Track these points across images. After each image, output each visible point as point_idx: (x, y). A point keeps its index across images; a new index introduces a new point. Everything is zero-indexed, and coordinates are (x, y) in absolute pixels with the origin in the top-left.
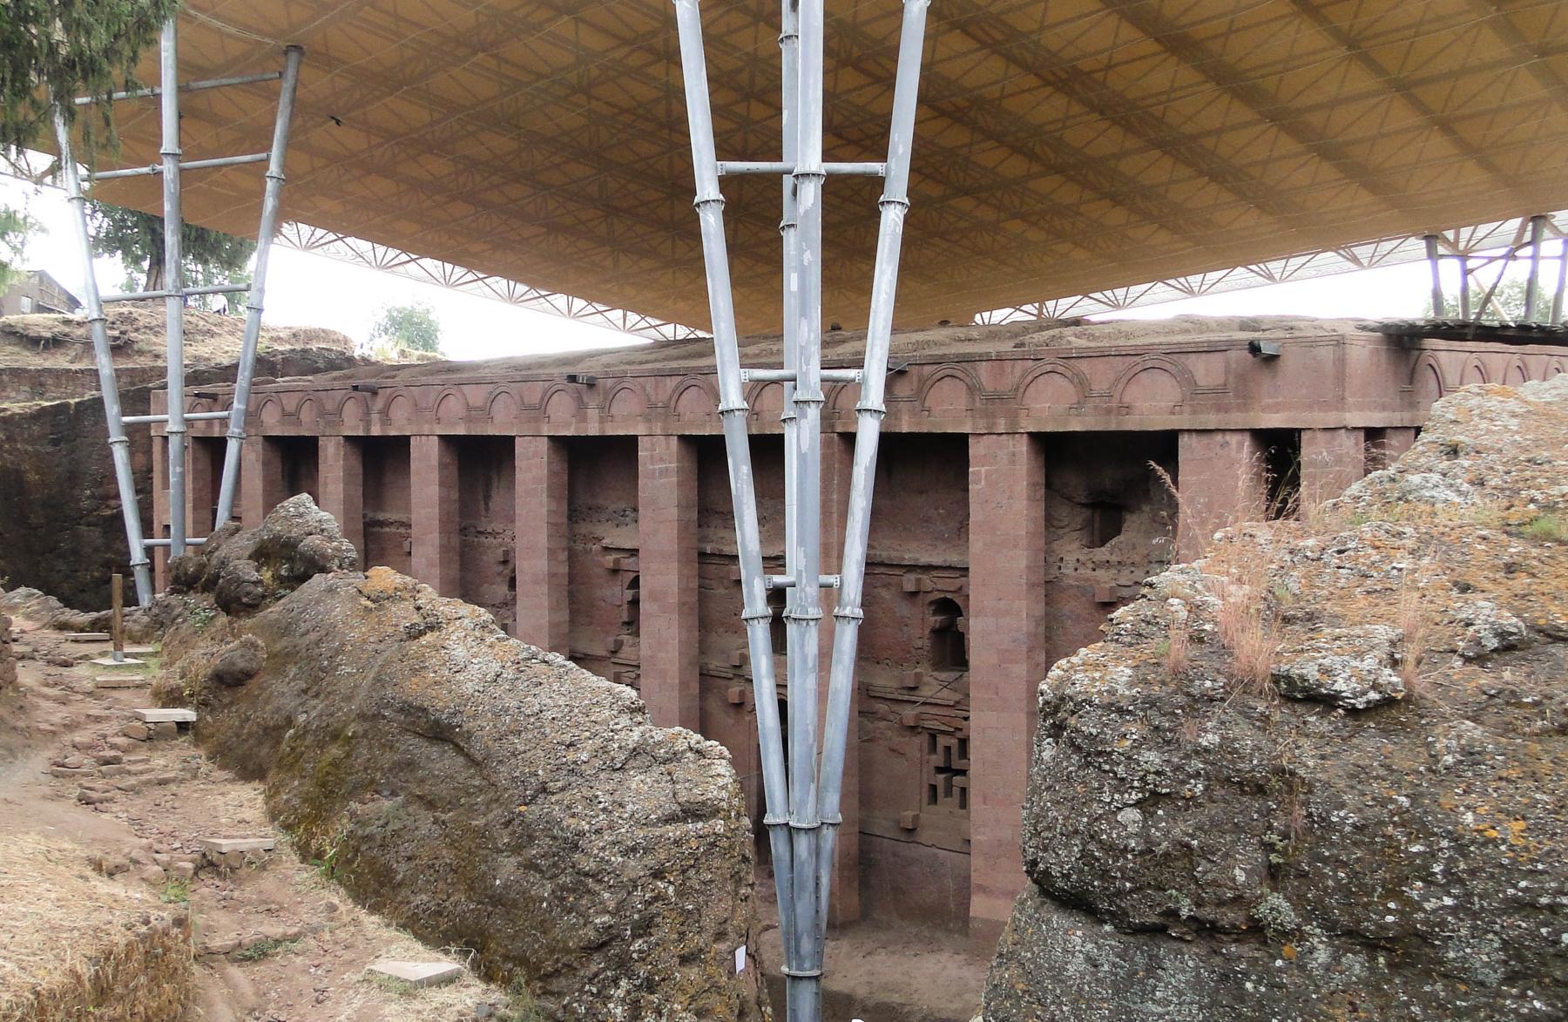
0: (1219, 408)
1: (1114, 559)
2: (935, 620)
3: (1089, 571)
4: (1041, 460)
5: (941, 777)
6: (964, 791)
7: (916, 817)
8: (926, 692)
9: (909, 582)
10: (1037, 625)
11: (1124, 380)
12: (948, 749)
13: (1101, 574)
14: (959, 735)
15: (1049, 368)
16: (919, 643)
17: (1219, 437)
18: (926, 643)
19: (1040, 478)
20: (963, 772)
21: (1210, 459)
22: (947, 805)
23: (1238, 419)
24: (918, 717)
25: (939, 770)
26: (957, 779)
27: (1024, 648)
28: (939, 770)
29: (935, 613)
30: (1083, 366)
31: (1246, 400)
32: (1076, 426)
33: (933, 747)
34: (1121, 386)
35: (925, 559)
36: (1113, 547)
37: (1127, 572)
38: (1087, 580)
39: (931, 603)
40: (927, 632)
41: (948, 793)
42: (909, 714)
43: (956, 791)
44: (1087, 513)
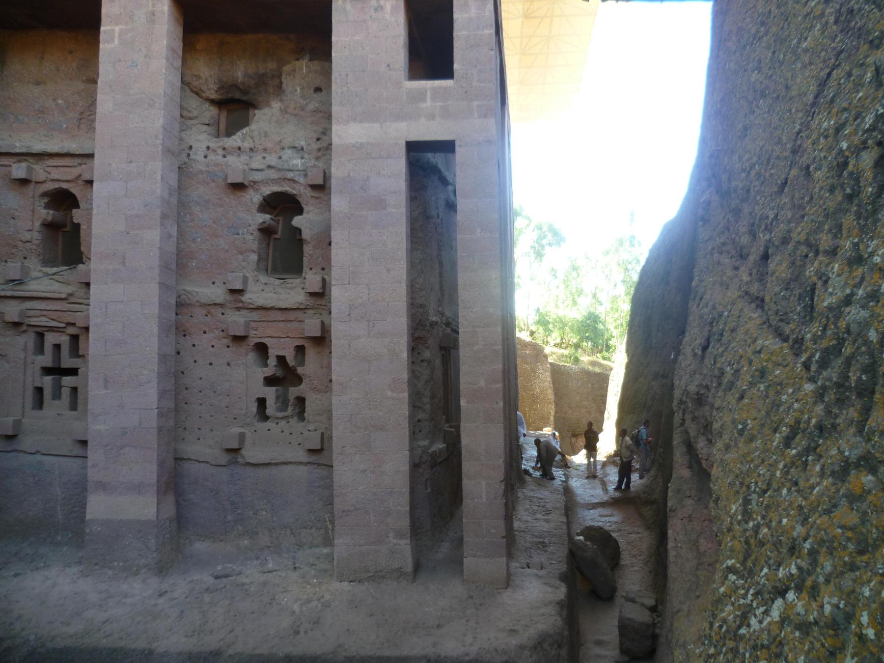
1: (246, 145)
2: (47, 214)
3: (220, 158)
4: (180, 30)
5: (48, 380)
6: (74, 390)
7: (17, 424)
8: (35, 287)
9: (19, 170)
10: (170, 194)
12: (57, 347)
13: (232, 160)
14: (72, 330)
16: (28, 236)
18: (36, 236)
19: (179, 45)
20: (73, 372)
21: (365, 21)
22: (54, 409)
24: (22, 313)
25: (47, 371)
26: (67, 381)
27: (158, 213)
28: (47, 371)
29: (47, 206)
33: (40, 349)
35: (38, 147)
36: (244, 135)
37: (259, 158)
39: (44, 195)
40: (37, 224)
41: (57, 395)
43: (66, 392)
44: (213, 111)
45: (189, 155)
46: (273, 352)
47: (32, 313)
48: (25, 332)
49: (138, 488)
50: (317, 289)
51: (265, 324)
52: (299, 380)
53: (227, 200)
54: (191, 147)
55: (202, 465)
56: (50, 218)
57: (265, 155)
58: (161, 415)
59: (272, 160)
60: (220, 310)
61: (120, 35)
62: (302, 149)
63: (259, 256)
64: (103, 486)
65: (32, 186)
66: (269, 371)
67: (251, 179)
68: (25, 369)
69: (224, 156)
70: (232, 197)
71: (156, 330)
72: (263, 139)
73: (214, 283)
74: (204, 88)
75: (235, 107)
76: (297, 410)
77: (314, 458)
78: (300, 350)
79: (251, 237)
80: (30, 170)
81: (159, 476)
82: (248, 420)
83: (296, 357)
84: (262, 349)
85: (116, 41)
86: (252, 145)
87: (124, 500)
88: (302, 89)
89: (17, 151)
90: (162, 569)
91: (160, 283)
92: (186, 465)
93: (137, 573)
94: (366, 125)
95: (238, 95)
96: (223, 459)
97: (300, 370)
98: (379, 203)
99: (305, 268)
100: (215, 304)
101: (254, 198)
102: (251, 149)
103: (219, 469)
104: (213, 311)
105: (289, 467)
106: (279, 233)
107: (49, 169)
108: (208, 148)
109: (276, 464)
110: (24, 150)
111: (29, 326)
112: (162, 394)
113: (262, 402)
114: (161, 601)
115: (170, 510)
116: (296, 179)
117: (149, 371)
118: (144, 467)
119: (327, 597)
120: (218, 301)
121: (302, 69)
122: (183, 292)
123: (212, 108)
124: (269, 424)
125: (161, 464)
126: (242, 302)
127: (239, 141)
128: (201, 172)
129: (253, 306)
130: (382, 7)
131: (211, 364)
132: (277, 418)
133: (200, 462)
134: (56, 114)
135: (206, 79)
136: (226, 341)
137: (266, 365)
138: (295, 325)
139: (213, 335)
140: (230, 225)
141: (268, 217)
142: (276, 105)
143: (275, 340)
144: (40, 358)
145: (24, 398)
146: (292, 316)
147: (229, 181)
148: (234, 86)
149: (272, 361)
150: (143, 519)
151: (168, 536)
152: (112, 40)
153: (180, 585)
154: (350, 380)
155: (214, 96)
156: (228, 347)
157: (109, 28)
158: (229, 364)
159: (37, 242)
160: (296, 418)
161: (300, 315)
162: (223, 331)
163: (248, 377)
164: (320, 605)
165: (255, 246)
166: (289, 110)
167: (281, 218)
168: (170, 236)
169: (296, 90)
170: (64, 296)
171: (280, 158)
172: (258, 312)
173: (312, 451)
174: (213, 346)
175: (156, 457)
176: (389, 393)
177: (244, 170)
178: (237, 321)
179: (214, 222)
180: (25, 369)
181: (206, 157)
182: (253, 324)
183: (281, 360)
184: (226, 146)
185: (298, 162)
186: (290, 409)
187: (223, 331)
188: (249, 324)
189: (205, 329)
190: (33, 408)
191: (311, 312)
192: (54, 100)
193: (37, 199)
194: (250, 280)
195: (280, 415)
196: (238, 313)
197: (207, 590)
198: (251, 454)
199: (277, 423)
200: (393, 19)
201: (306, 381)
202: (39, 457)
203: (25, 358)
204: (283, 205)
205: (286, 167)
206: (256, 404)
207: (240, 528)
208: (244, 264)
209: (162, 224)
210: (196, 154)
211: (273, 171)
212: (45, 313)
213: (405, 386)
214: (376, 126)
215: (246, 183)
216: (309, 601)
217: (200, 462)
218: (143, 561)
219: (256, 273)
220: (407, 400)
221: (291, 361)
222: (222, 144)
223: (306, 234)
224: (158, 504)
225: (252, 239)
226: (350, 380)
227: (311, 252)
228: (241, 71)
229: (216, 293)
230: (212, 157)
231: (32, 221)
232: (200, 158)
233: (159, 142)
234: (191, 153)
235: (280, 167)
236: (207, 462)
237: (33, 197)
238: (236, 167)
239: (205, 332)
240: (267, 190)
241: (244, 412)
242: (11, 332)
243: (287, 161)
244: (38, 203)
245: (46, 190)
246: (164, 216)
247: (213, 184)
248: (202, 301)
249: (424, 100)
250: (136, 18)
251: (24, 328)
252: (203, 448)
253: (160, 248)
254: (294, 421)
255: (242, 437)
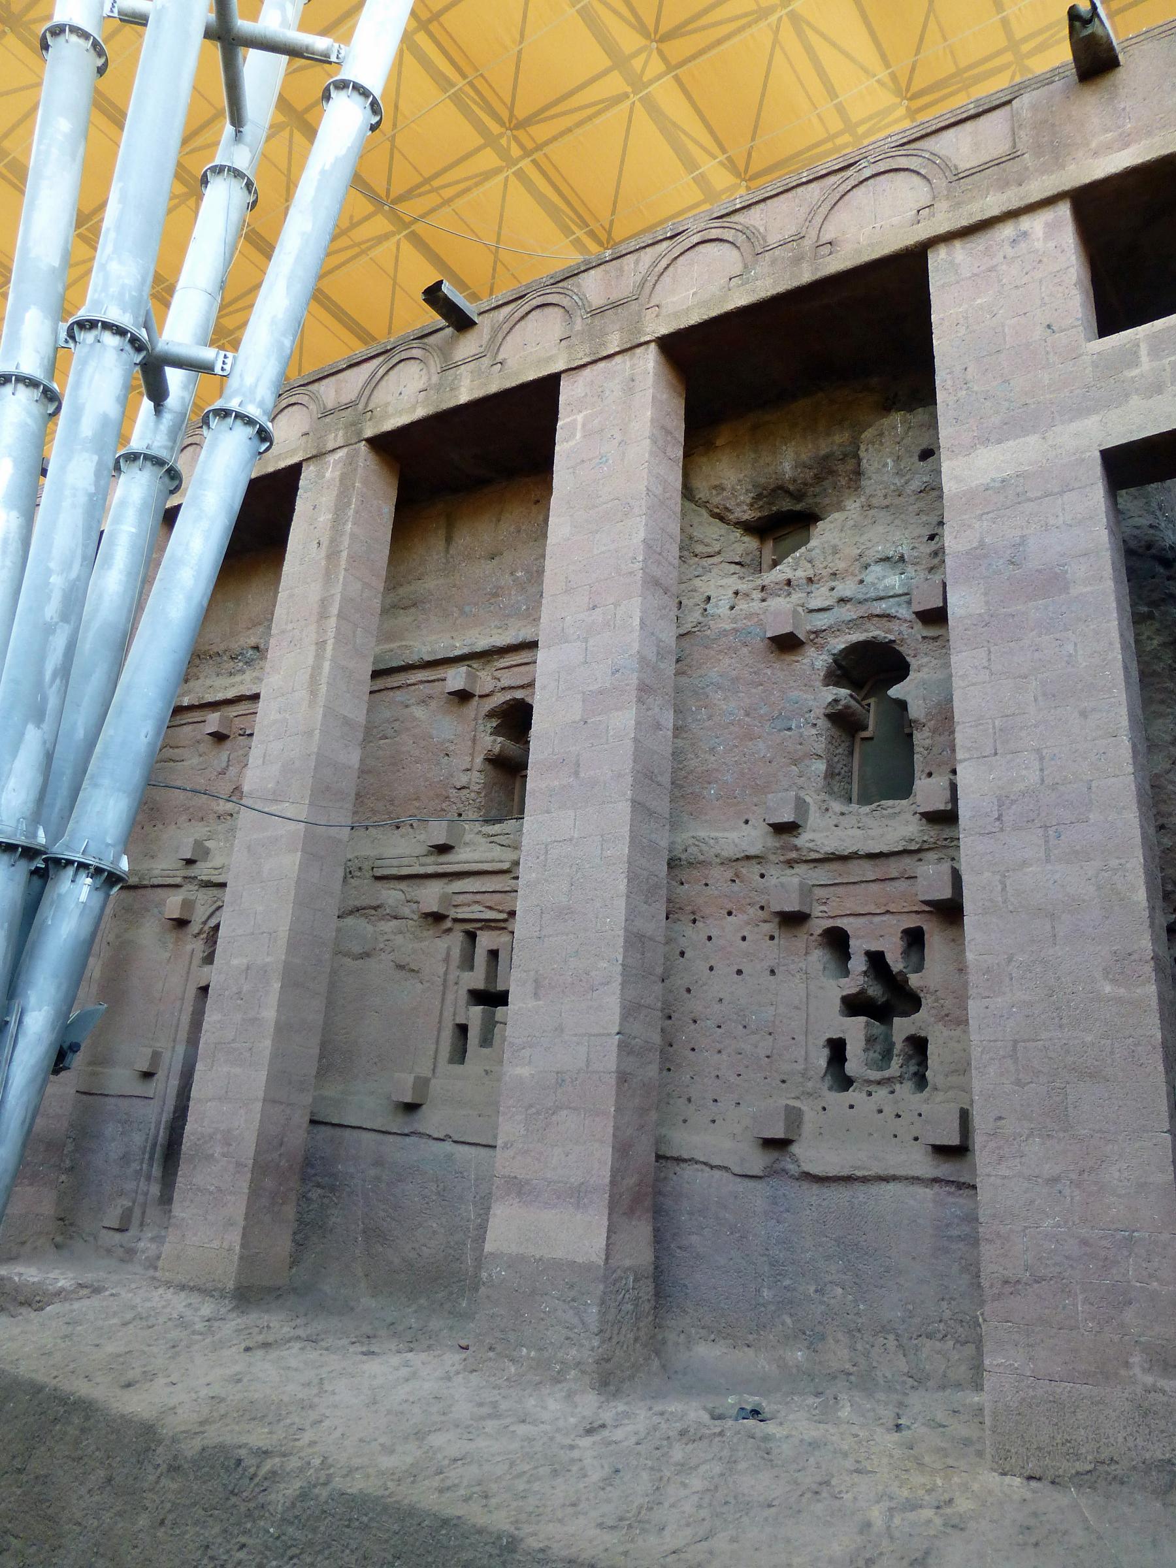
0: (1003, 185)
2: (491, 743)
5: (477, 1010)
7: (422, 1084)
8: (463, 858)
9: (456, 678)
10: (661, 656)
11: (824, 210)
15: (696, 239)
16: (463, 779)
17: (1007, 231)
18: (476, 779)
23: (1037, 189)
27: (634, 680)
29: (496, 732)
30: (754, 218)
31: (1056, 151)
32: (740, 299)
33: (468, 962)
34: (818, 220)
37: (824, 590)
38: (749, 616)
39: (491, 715)
40: (479, 760)
42: (431, 896)
45: (705, 610)
46: (858, 946)
47: (460, 899)
48: (449, 930)
49: (577, 1195)
50: (939, 803)
51: (840, 890)
52: (911, 1002)
53: (769, 672)
54: (709, 598)
55: (717, 1174)
56: (497, 749)
57: (833, 584)
58: (625, 1048)
59: (847, 588)
60: (757, 869)
61: (584, 425)
62: (902, 558)
63: (830, 766)
64: (518, 1188)
65: (475, 702)
66: (852, 985)
67: (809, 628)
68: (444, 994)
69: (764, 600)
70: (777, 665)
71: (622, 886)
72: (830, 558)
73: (747, 822)
74: (730, 504)
75: (782, 522)
76: (913, 1068)
77: (945, 1169)
78: (914, 939)
79: (814, 731)
80: (471, 677)
81: (617, 1175)
82: (810, 1084)
83: (906, 953)
84: (837, 942)
85: (578, 435)
86: (810, 573)
87: (550, 1214)
88: (898, 459)
89: (458, 653)
90: (608, 1380)
91: (633, 801)
92: (688, 1171)
93: (557, 1380)
94: (1011, 443)
95: (786, 505)
96: (757, 1161)
97: (914, 980)
98: (1052, 582)
99: (917, 774)
100: (748, 858)
101: (817, 660)
102: (810, 580)
103: (751, 1184)
104: (744, 871)
105: (891, 1187)
106: (871, 728)
107: (498, 674)
108: (736, 593)
109: (865, 1180)
110: (466, 650)
111: (456, 920)
112: (630, 1010)
113: (837, 1049)
114: (586, 1442)
115: (638, 1250)
116: (893, 611)
117: (608, 962)
118: (584, 1151)
119: (963, 1505)
120: (752, 851)
121: (895, 428)
122: (691, 841)
123: (746, 539)
124: (854, 1095)
125: (622, 1150)
126: (796, 848)
127: (788, 570)
128: (724, 633)
129: (814, 856)
130: (1025, 234)
131: (739, 972)
132: (869, 1082)
133: (712, 1167)
134: (513, 592)
135: (733, 488)
136: (768, 928)
137: (846, 973)
138: (902, 885)
139: (745, 917)
140: (776, 713)
141: (844, 692)
142: (853, 506)
143: (862, 920)
144: (466, 975)
145: (437, 1042)
146: (893, 868)
147: (769, 635)
148: (780, 490)
149: (858, 964)
150: (580, 1260)
151: (629, 1307)
152: (573, 435)
153: (634, 1419)
154: (1010, 960)
155: (748, 515)
156: (772, 938)
157: (568, 420)
158: (773, 972)
159: (476, 788)
160: (909, 1085)
161: (907, 862)
162: (762, 908)
163: (813, 998)
164: (938, 1521)
165: (820, 746)
166: (874, 501)
167: (872, 701)
168: (658, 726)
169: (885, 465)
170: (506, 866)
171: (862, 582)
172: (828, 866)
173: (942, 1151)
174: (744, 939)
175: (610, 1130)
176: (1108, 989)
177: (795, 612)
178: (786, 887)
179: (748, 715)
180: (444, 994)
181: (732, 608)
182: (820, 893)
183: (876, 960)
184: (765, 583)
185: (893, 581)
186: (896, 1063)
187: (762, 908)
188: (810, 891)
189: (729, 906)
190: (451, 1061)
191: (932, 856)
192: (512, 574)
193: (480, 721)
194: (813, 808)
195: (876, 1075)
196: (789, 872)
197: (683, 1433)
198: (812, 1154)
199: (870, 1094)
200: (1051, 245)
201: (927, 1002)
202: (448, 1146)
203: (446, 974)
204: (871, 667)
205: (873, 594)
206: (826, 1052)
207: (788, 1321)
208: (800, 781)
209: (640, 700)
210: (717, 606)
211: (848, 606)
212: (478, 897)
213: (1148, 969)
214: (1033, 439)
215: (802, 636)
216: (913, 1506)
217: (712, 1167)
218: (574, 1352)
219: (823, 796)
220: (1154, 1003)
221: (896, 963)
222: (759, 582)
223: (916, 710)
224: (611, 1231)
225: (815, 736)
226: (1010, 960)
227: (928, 742)
228: (788, 461)
229: (752, 837)
230: (742, 605)
231: (472, 755)
232: (723, 610)
233: (638, 565)
234: (708, 607)
235: (861, 596)
236: (726, 1169)
237: (475, 719)
238: (780, 613)
239: (730, 913)
240: (839, 643)
241: (800, 1067)
242: (431, 932)
243: (873, 584)
244: (482, 728)
245: (492, 706)
246: (644, 689)
247: (745, 650)
248: (725, 854)
249: (1134, 362)
250: (607, 393)
251: (448, 924)
252: (717, 1139)
253: (636, 740)
254: (905, 1090)
255: (794, 1117)
